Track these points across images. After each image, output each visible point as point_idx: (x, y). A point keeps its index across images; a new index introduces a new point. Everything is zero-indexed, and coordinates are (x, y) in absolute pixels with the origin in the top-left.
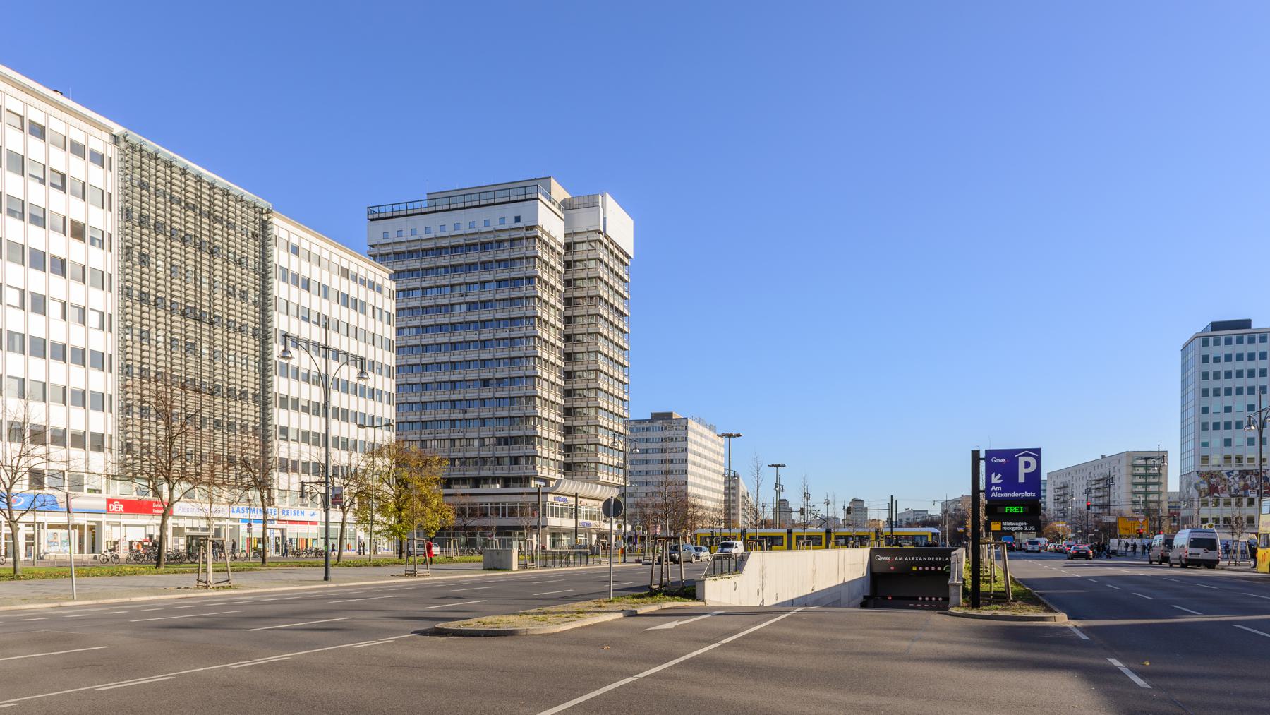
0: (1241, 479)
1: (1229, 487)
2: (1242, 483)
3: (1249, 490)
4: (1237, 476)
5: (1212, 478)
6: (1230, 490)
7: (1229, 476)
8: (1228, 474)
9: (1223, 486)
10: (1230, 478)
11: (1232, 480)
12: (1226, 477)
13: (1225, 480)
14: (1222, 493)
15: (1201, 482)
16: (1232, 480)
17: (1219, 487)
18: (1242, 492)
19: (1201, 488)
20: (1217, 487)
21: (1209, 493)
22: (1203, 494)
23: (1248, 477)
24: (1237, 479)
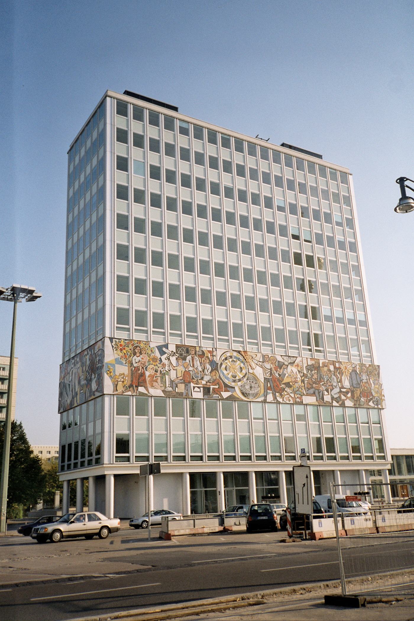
0: (181, 362)
1: (163, 375)
2: (181, 369)
3: (192, 385)
4: (173, 354)
5: (135, 354)
6: (164, 382)
7: (162, 353)
8: (160, 348)
9: (153, 372)
10: (163, 357)
11: (166, 362)
12: (157, 354)
13: (155, 359)
14: (152, 386)
15: (118, 362)
16: (166, 362)
17: (147, 373)
18: (181, 388)
19: (117, 373)
20: (143, 375)
21: (131, 386)
22: (120, 389)
23: (189, 358)
24: (173, 359)
